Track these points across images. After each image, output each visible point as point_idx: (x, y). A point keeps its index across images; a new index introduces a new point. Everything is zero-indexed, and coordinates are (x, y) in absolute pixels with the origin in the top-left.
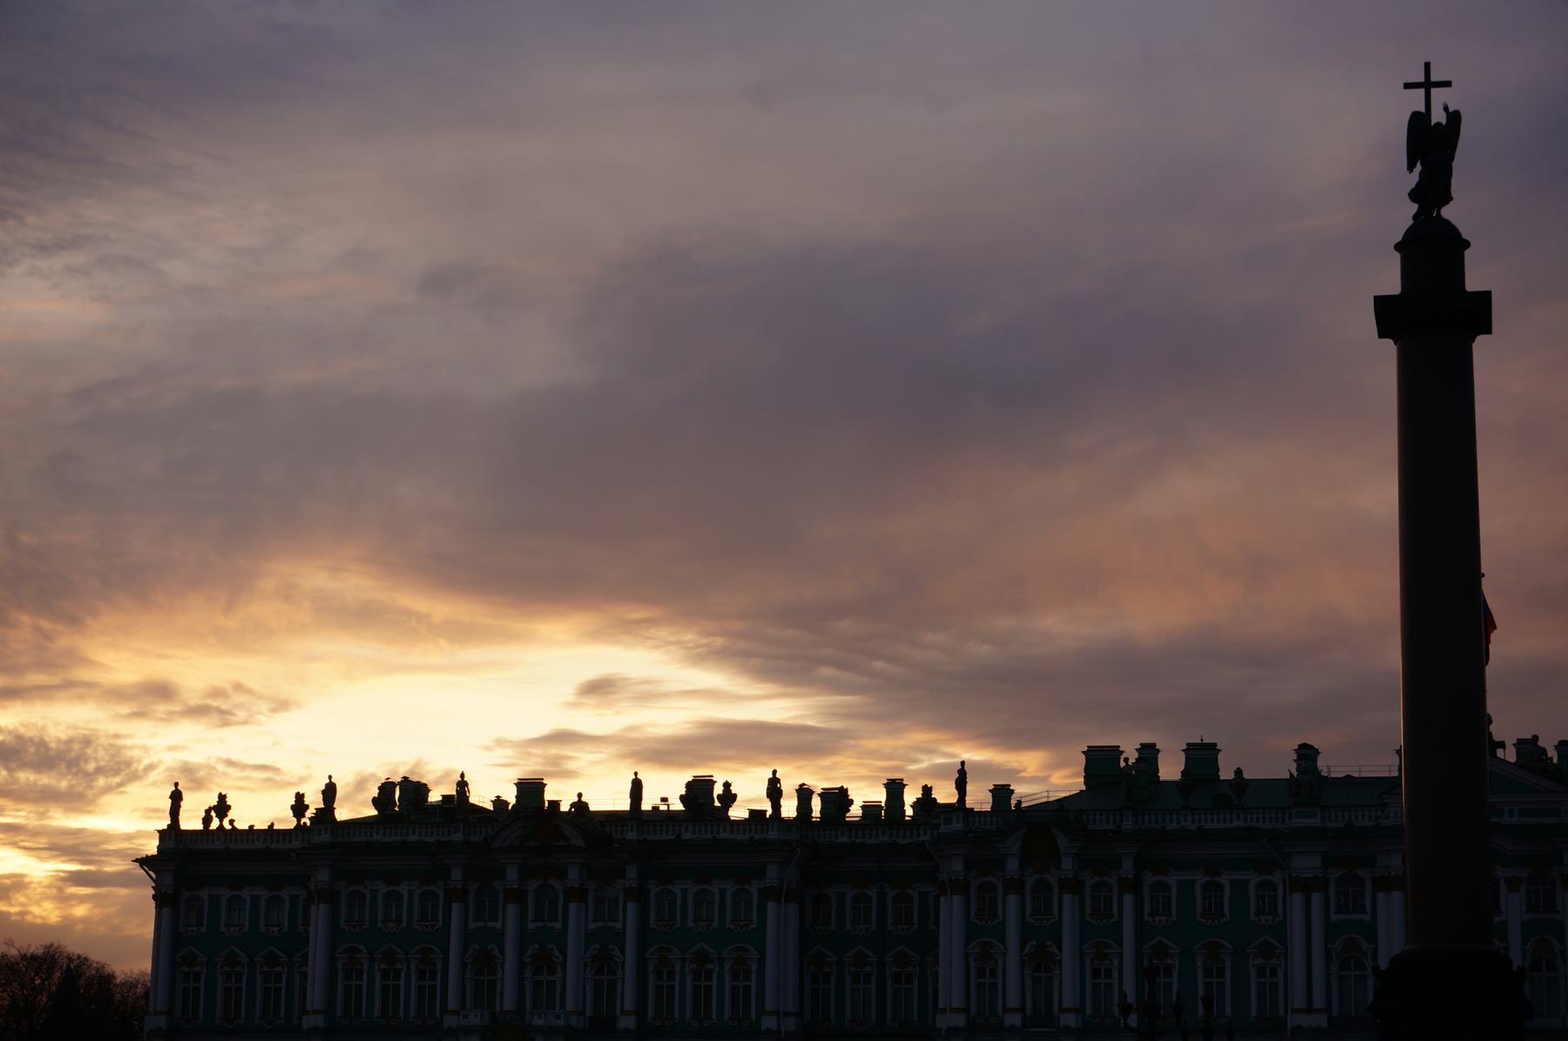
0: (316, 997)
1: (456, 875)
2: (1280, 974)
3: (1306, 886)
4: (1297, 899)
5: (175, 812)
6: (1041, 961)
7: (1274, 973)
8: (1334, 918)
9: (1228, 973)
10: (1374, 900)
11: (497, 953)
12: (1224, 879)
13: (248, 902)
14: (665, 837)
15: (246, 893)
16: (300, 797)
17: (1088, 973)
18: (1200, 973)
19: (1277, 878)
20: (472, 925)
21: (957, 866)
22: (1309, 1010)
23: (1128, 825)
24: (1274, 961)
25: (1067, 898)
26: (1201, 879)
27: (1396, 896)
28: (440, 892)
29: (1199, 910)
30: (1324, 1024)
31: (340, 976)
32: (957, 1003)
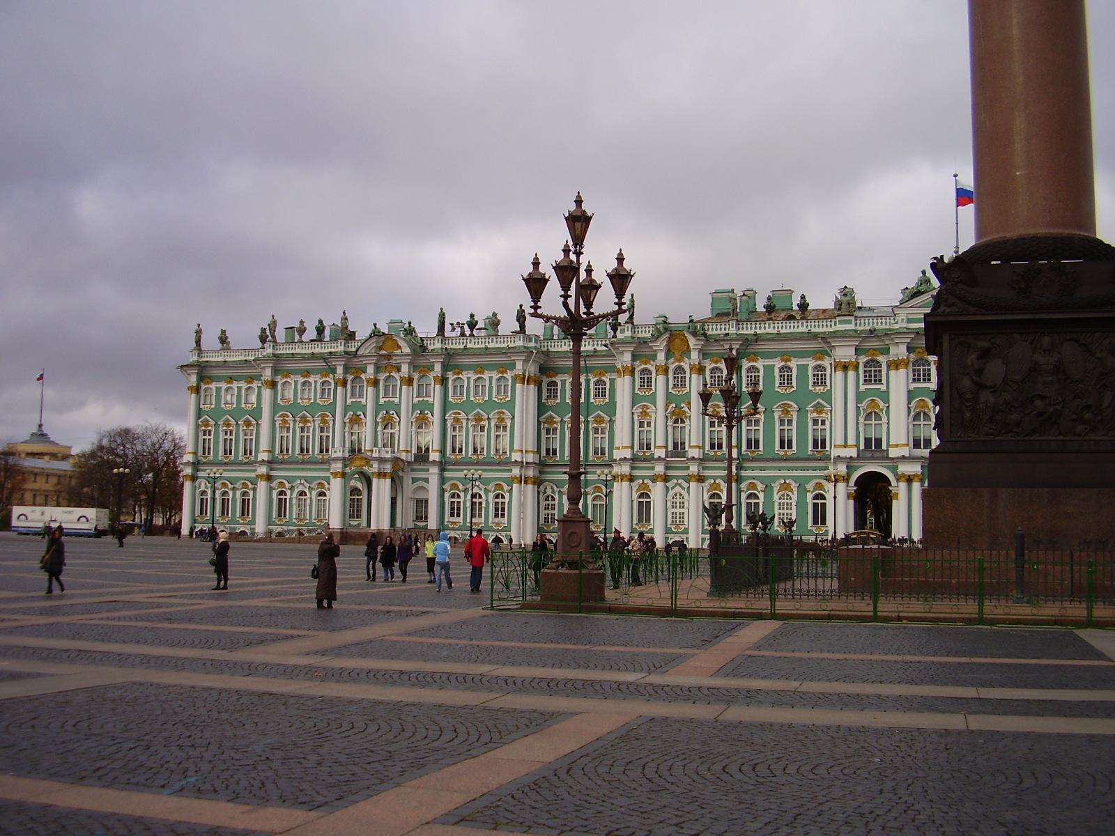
0: (264, 444)
1: (340, 370)
2: (827, 423)
3: (845, 368)
4: (840, 374)
5: (198, 342)
6: (679, 417)
7: (823, 422)
8: (862, 388)
9: (794, 423)
10: (888, 375)
11: (362, 416)
12: (793, 364)
13: (236, 390)
14: (458, 347)
15: (235, 385)
16: (263, 330)
17: (707, 424)
18: (777, 423)
19: (826, 363)
20: (349, 401)
21: (627, 357)
22: (845, 446)
23: (733, 331)
24: (824, 415)
25: (694, 377)
26: (778, 364)
27: (902, 371)
28: (332, 382)
29: (777, 384)
30: (855, 455)
31: (278, 430)
32: (627, 443)
